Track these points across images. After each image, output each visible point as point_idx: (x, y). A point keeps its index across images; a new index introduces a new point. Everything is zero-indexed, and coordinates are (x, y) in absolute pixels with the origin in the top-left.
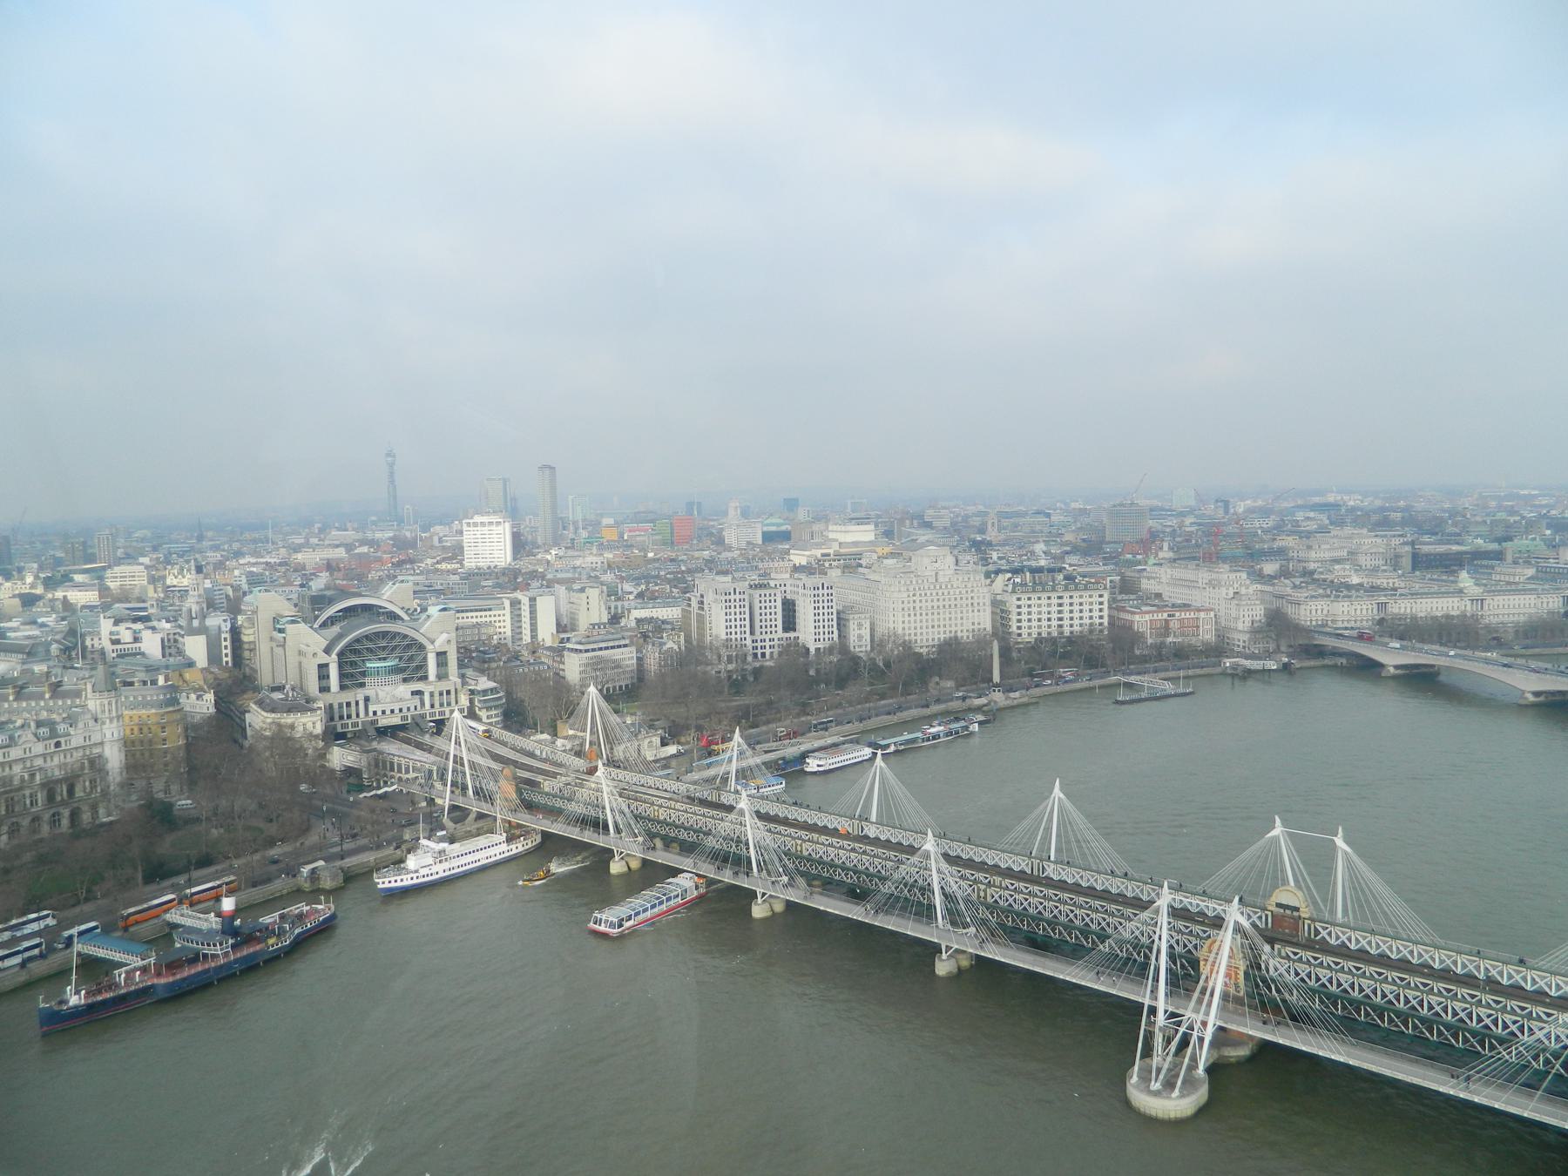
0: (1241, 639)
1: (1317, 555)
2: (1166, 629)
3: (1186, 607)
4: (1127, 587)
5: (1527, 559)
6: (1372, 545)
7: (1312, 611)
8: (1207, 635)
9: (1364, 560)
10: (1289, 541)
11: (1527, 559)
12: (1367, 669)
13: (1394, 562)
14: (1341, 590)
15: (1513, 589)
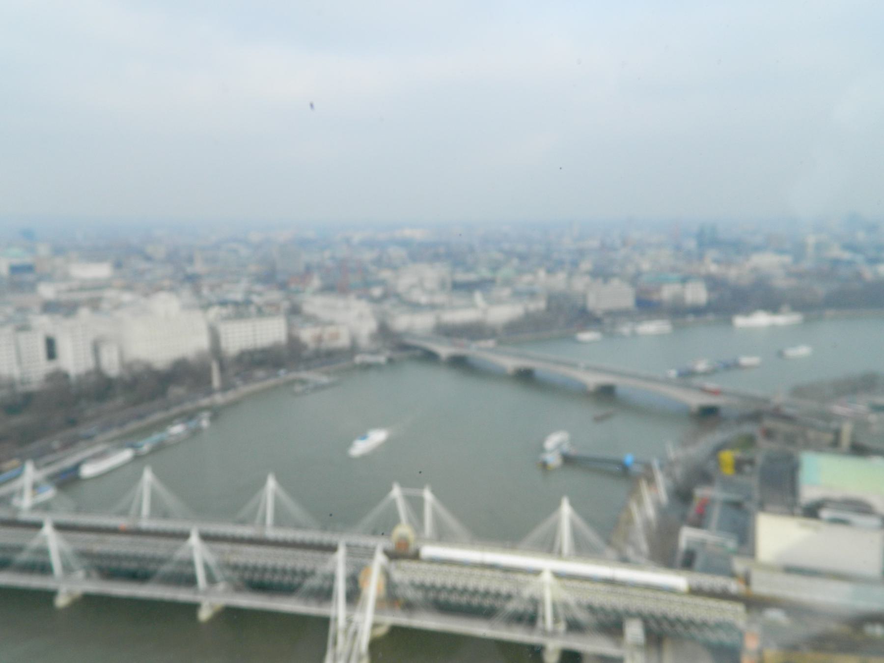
0: (364, 341)
1: (404, 282)
2: (319, 339)
3: (331, 323)
4: (295, 311)
5: (507, 283)
6: (432, 274)
7: (402, 322)
8: (343, 341)
9: (429, 285)
10: (386, 274)
11: (507, 283)
12: (430, 357)
13: (442, 285)
14: (415, 307)
15: (500, 302)
